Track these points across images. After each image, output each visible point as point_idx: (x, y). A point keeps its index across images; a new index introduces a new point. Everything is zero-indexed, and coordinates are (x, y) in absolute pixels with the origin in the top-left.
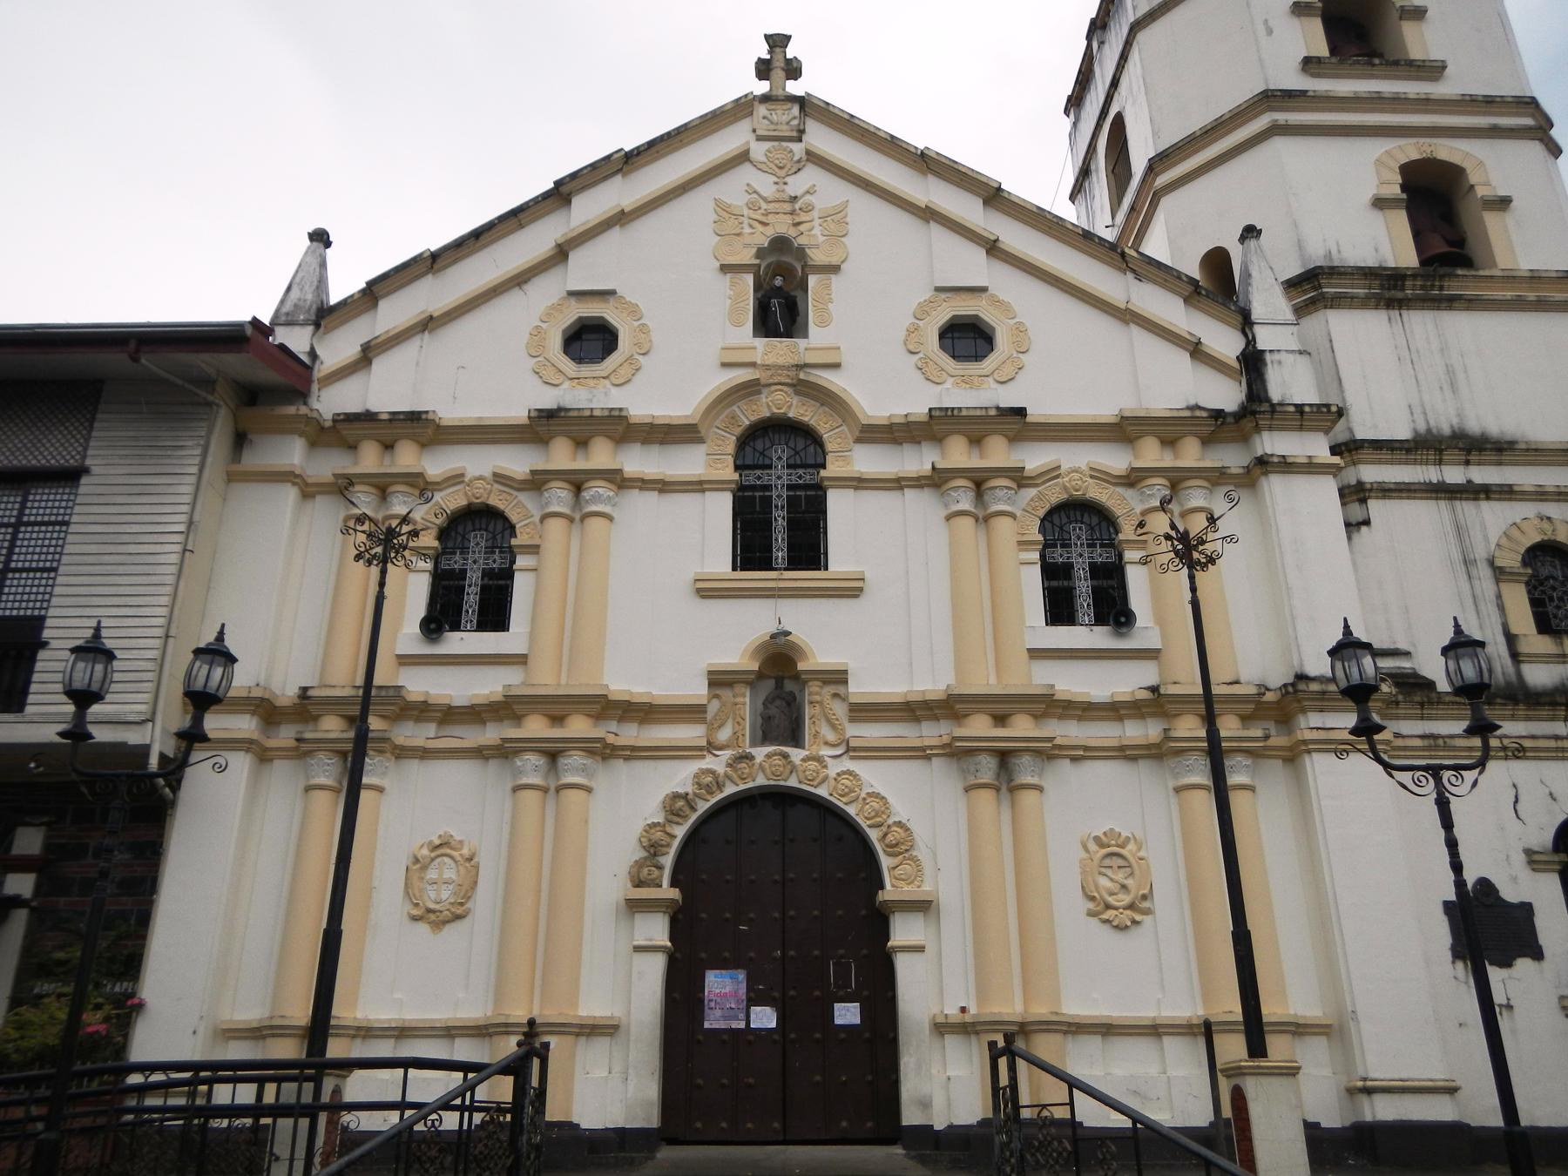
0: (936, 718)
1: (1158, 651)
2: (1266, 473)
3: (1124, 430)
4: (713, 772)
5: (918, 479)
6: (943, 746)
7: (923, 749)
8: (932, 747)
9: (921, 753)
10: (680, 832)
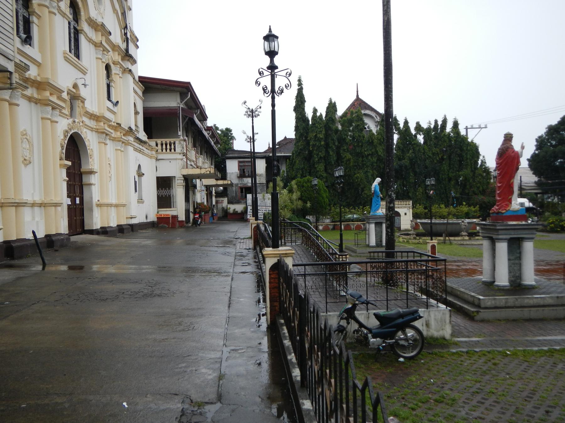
0: (94, 120)
1: (115, 113)
2: (128, 73)
3: (115, 47)
4: (70, 124)
5: (94, 41)
6: (96, 129)
7: (92, 128)
8: (94, 128)
9: (92, 129)
10: (66, 142)
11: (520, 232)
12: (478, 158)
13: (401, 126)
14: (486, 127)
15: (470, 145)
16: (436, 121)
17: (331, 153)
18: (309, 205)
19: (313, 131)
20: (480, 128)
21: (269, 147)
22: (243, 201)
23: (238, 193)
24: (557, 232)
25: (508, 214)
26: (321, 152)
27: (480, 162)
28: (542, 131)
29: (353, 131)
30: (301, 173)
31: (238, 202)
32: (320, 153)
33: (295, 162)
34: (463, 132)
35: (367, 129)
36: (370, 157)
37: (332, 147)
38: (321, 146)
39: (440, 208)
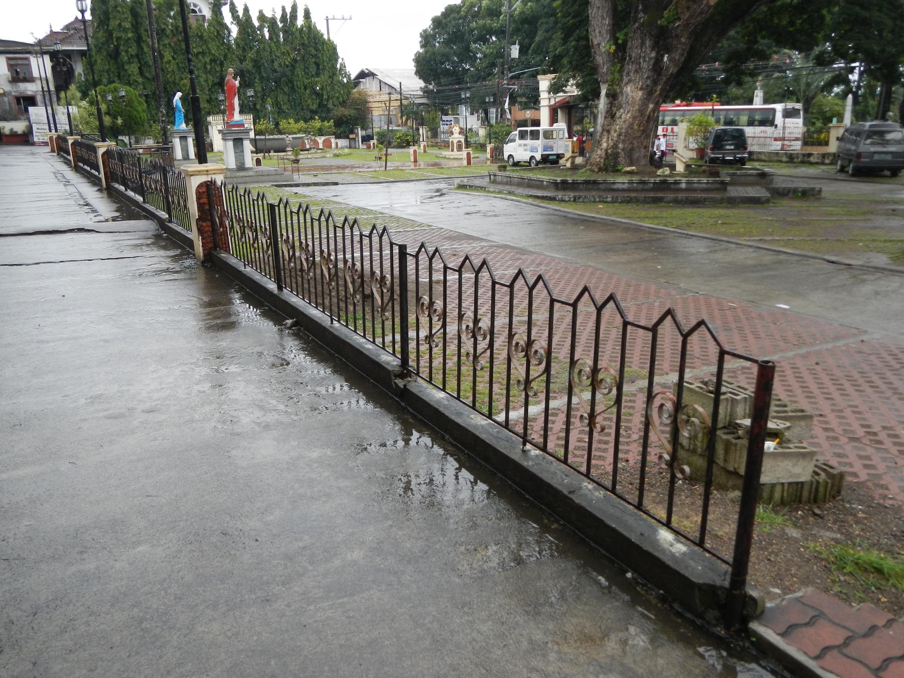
11: (240, 134)
12: (337, 60)
13: (241, 13)
14: (351, 19)
15: (327, 44)
16: (284, 9)
17: (146, 49)
18: (120, 121)
19: (115, 17)
20: (343, 19)
21: (51, 31)
22: (22, 117)
23: (13, 105)
24: (404, 147)
25: (232, 123)
26: (131, 47)
27: (338, 66)
28: (426, 24)
29: (174, 18)
30: (107, 76)
31: (15, 118)
32: (130, 50)
33: (96, 61)
34: (321, 27)
35: (198, 14)
36: (200, 57)
37: (146, 41)
38: (129, 39)
39: (289, 123)
